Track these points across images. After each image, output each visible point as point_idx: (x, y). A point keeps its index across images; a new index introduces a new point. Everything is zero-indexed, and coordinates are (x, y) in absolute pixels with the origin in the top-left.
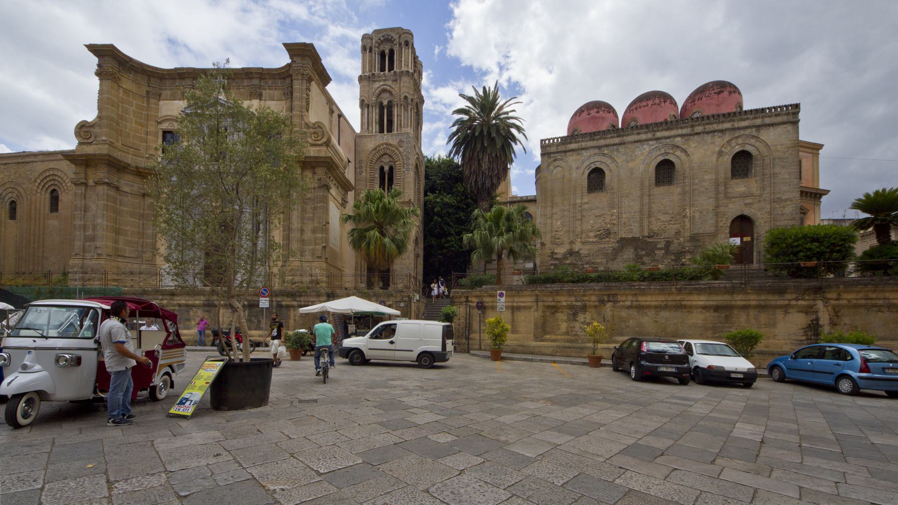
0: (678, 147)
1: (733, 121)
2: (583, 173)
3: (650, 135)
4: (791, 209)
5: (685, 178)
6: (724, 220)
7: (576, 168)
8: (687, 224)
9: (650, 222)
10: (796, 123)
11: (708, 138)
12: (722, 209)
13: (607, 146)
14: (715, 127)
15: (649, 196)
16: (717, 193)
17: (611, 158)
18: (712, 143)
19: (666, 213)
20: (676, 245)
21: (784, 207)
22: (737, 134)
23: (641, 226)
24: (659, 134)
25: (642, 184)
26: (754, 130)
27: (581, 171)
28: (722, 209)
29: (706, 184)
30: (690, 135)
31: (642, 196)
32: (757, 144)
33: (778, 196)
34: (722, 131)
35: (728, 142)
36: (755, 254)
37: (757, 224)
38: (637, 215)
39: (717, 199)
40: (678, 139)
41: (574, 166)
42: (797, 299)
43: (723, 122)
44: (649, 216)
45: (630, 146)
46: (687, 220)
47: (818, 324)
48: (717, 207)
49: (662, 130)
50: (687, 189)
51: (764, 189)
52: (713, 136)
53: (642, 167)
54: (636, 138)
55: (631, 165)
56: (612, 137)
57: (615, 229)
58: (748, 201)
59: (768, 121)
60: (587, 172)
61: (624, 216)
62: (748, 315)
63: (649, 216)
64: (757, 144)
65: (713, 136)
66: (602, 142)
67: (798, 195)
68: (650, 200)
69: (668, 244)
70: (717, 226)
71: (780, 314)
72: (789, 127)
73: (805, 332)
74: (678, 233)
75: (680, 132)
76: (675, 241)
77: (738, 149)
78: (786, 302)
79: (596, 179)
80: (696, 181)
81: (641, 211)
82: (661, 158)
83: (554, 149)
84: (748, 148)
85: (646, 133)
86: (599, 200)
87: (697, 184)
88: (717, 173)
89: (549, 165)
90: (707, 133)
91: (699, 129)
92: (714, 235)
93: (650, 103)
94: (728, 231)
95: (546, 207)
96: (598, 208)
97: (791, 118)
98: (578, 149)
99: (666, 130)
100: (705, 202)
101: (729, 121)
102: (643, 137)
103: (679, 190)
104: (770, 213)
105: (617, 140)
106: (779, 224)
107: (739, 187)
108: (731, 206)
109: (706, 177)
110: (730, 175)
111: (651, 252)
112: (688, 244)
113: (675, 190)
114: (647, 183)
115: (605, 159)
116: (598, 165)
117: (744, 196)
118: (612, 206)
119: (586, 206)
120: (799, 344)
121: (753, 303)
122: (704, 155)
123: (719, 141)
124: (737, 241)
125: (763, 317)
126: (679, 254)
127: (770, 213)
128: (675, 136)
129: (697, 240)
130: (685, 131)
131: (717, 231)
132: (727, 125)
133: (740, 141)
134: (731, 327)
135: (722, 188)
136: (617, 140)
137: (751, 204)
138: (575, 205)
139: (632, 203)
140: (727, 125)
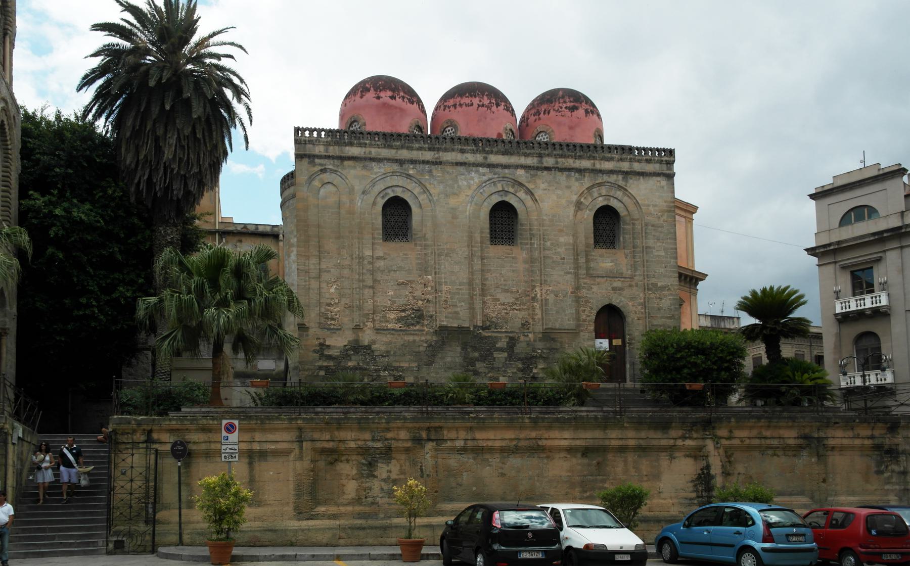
0: (521, 184)
1: (594, 158)
2: (374, 203)
3: (479, 158)
4: (668, 302)
5: (532, 236)
6: (588, 309)
7: (362, 189)
8: (538, 311)
9: (484, 302)
10: (670, 176)
11: (562, 177)
12: (584, 292)
13: (413, 162)
14: (570, 162)
15: (482, 258)
16: (577, 267)
17: (421, 184)
18: (568, 187)
19: (507, 291)
20: (524, 345)
21: (661, 299)
22: (599, 180)
23: (472, 308)
24: (494, 159)
25: (471, 238)
26: (620, 177)
27: (370, 198)
28: (584, 292)
29: (561, 250)
30: (538, 169)
31: (471, 257)
32: (625, 199)
33: (653, 281)
34: (580, 171)
35: (589, 189)
36: (628, 366)
37: (629, 320)
38: (465, 290)
39: (576, 275)
40: (521, 172)
41: (358, 187)
42: (684, 438)
43: (580, 157)
44: (484, 293)
45: (450, 169)
46: (537, 305)
47: (708, 473)
48: (577, 288)
49: (497, 153)
50: (536, 254)
51: (636, 269)
52: (568, 177)
53: (469, 209)
54: (460, 157)
55: (453, 202)
56: (420, 149)
57: (431, 310)
58: (617, 284)
59: (637, 167)
60: (381, 202)
61: (444, 288)
62: (625, 461)
63: (484, 293)
64: (625, 199)
65: (568, 177)
66: (405, 154)
67: (675, 281)
68: (483, 265)
69: (513, 342)
70: (578, 319)
71: (664, 461)
72: (663, 182)
73: (695, 486)
74: (525, 325)
75: (523, 160)
76: (522, 338)
77: (601, 202)
78: (672, 442)
79: (397, 217)
80: (548, 244)
81: (471, 283)
82: (496, 199)
83: (319, 150)
84: (614, 203)
85: (473, 152)
86: (400, 255)
87: (549, 249)
88: (575, 236)
89: (311, 179)
90: (561, 170)
91: (549, 162)
92: (574, 333)
93: (476, 101)
94: (592, 328)
95: (308, 258)
96: (400, 269)
97: (664, 168)
98: (365, 159)
99: (505, 153)
100: (561, 279)
101: (589, 158)
102: (470, 158)
103: (525, 254)
104: (644, 305)
105: (428, 156)
106: (655, 323)
107: (605, 260)
108: (595, 288)
109: (562, 240)
110: (592, 241)
111: (487, 356)
112: (540, 345)
113: (519, 253)
114: (477, 237)
115: (411, 185)
116: (399, 193)
117: (612, 276)
118: (424, 269)
119: (381, 264)
120: (690, 505)
121: (632, 443)
122: (556, 204)
123: (577, 186)
124: (604, 344)
125: (645, 465)
126: (529, 361)
127: (644, 305)
128: (517, 167)
129: (553, 339)
130: (531, 161)
131: (578, 326)
132: (586, 164)
133: (604, 191)
134: (604, 481)
135: (582, 260)
136: (428, 156)
137: (621, 289)
138: (361, 258)
139: (456, 268)
140: (586, 164)
